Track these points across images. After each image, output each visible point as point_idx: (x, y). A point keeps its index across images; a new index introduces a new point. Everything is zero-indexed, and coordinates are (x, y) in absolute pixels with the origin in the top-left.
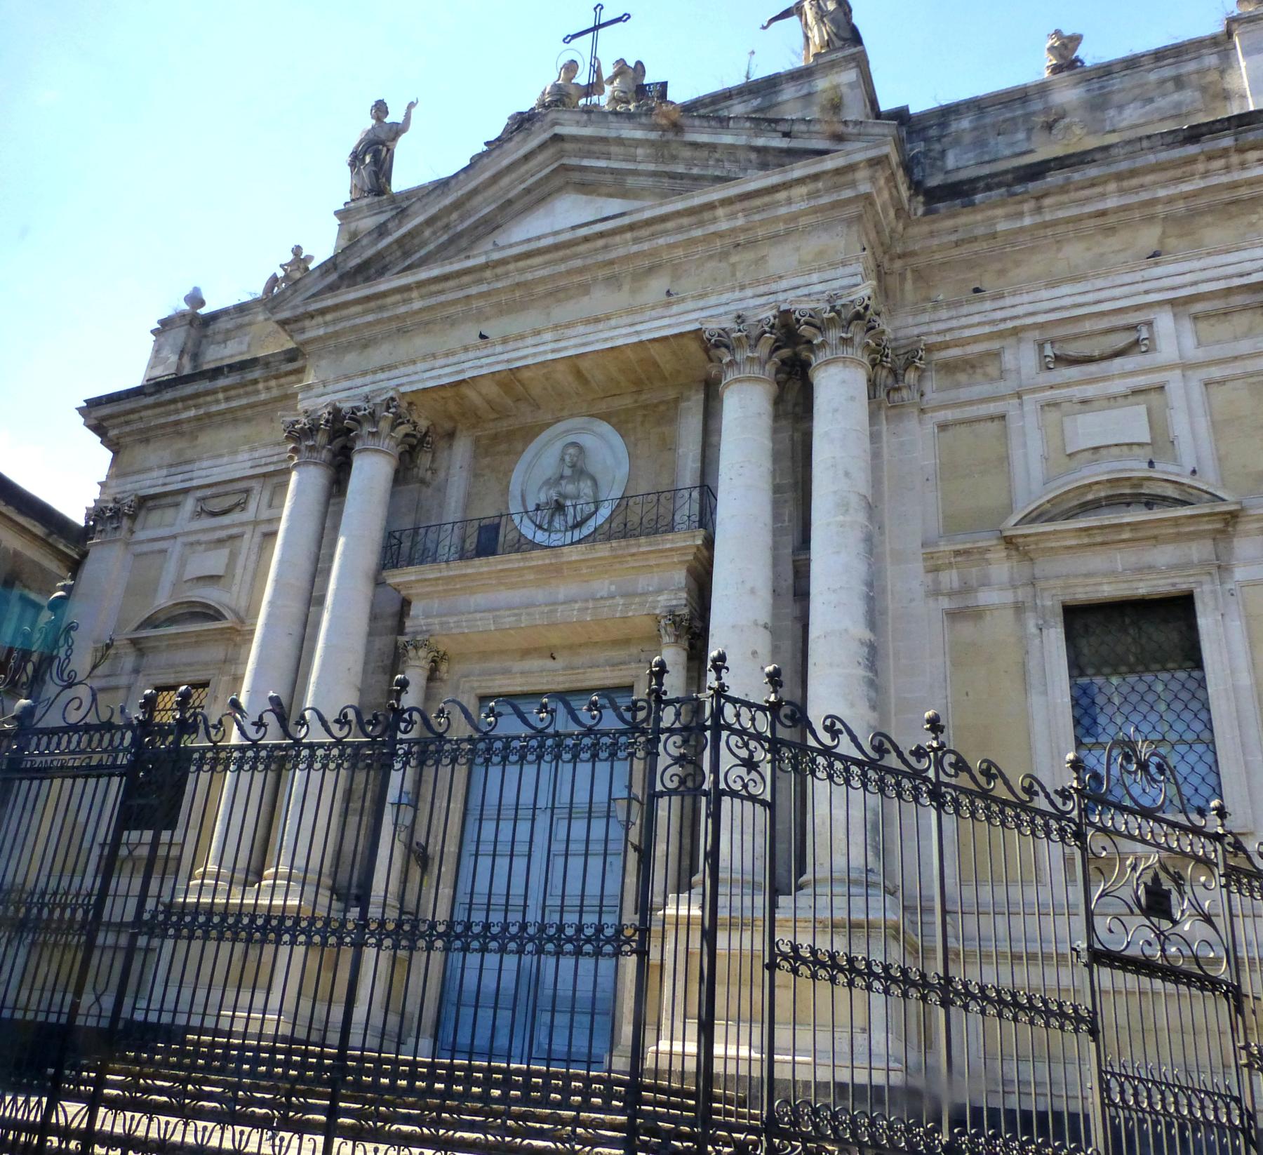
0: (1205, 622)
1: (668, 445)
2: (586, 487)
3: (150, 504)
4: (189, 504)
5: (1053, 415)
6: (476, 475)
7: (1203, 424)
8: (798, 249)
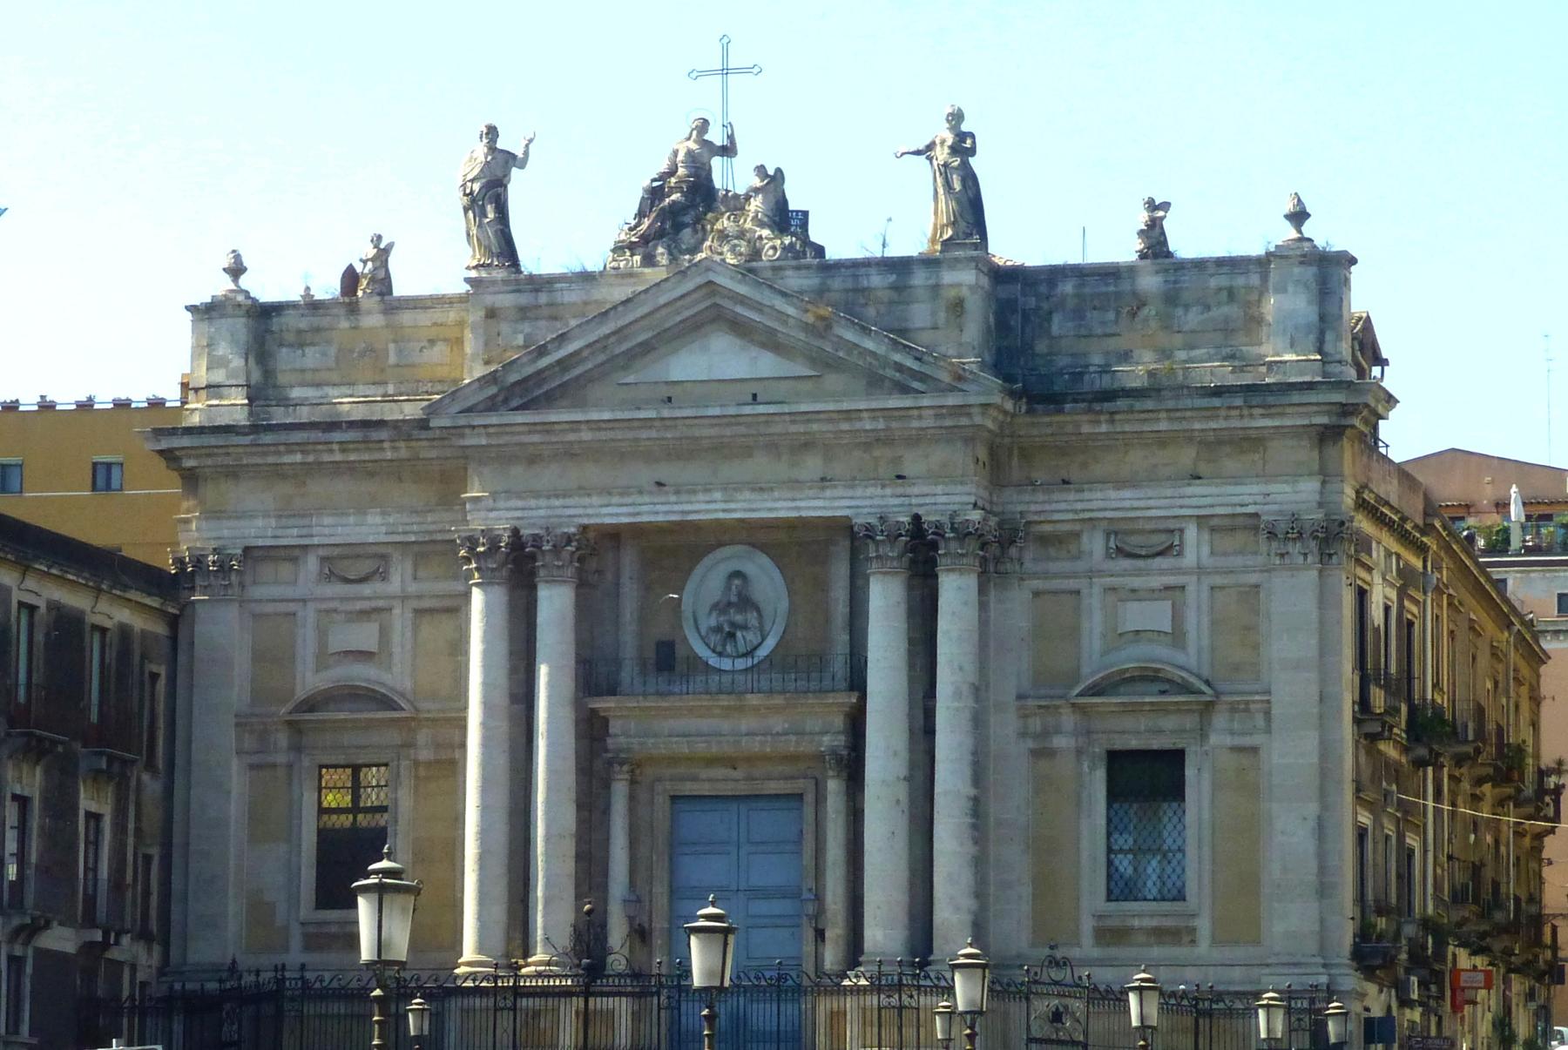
0: (1190, 772)
2: (752, 618)
4: (312, 563)
7: (1205, 620)
8: (927, 457)
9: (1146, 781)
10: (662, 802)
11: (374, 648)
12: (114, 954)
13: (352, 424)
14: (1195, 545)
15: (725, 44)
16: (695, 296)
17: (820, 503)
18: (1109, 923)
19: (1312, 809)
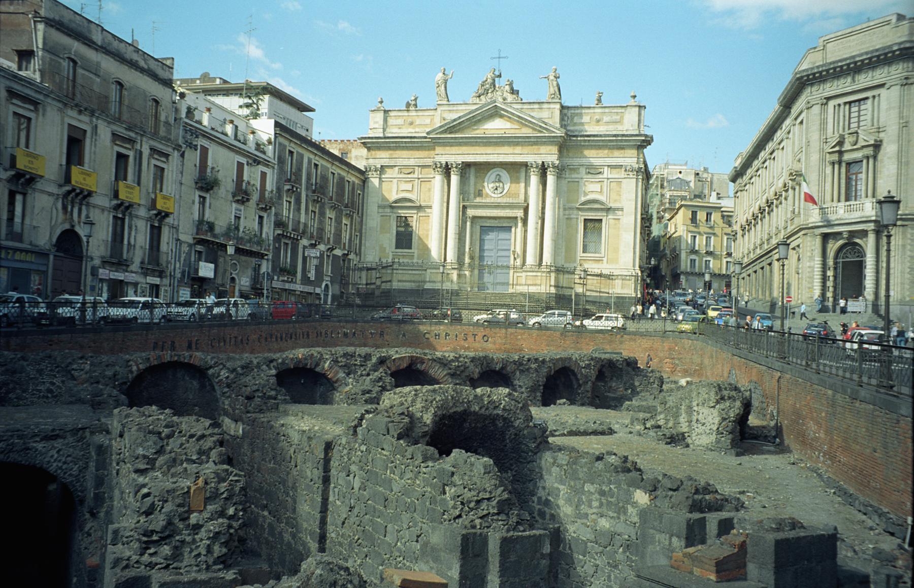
6: (476, 177)
9: (593, 225)
10: (478, 227)
12: (350, 257)
13: (408, 137)
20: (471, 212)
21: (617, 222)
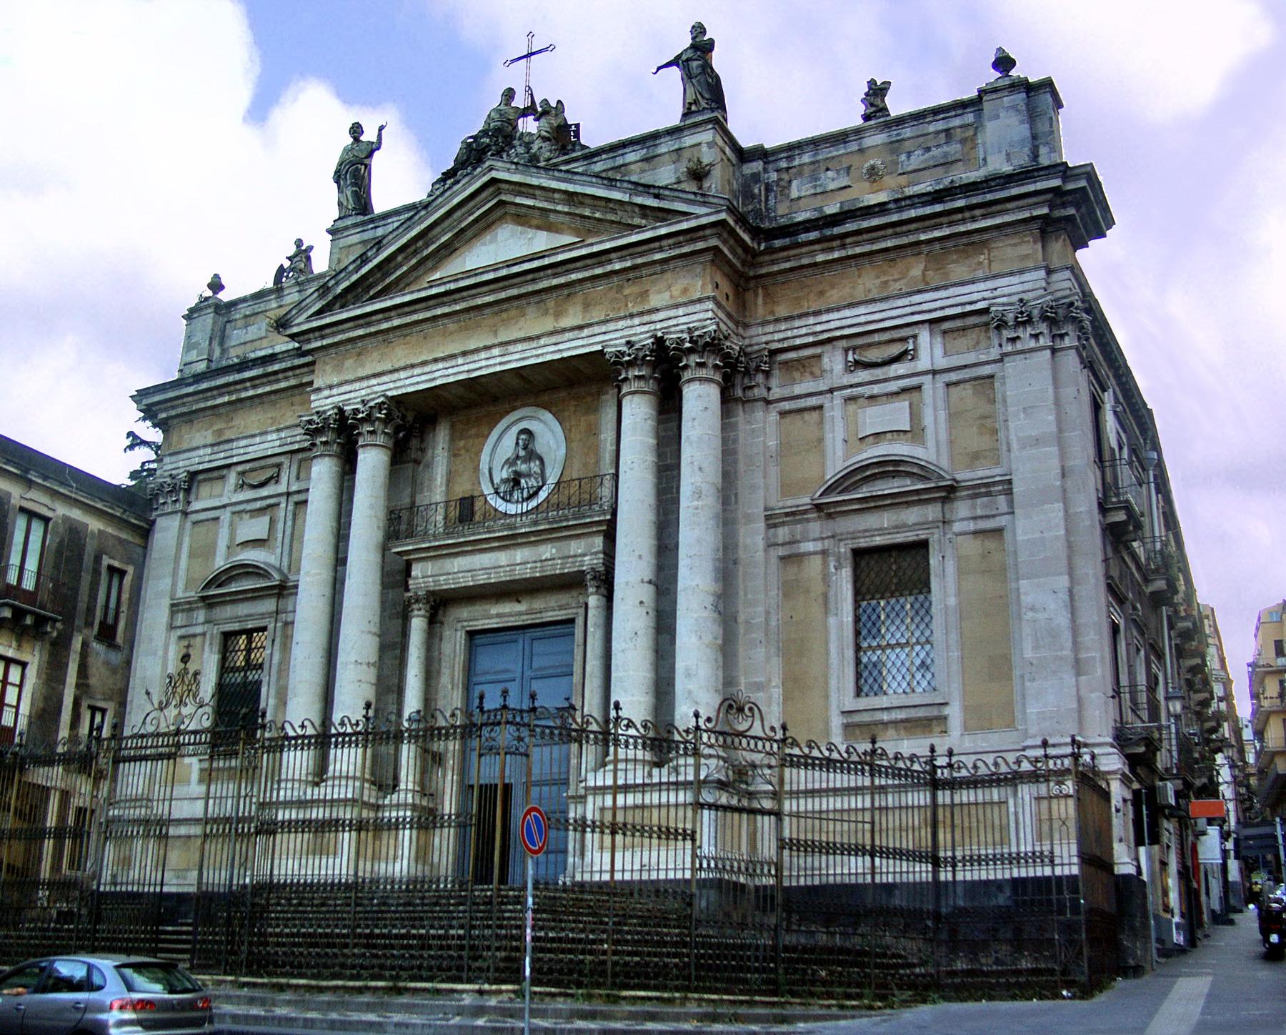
0: (934, 561)
1: (593, 431)
2: (535, 467)
3: (201, 477)
4: (232, 478)
5: (852, 407)
6: (454, 454)
7: (942, 415)
8: (669, 287)
11: (265, 537)
14: (930, 352)
15: (531, 35)
16: (483, 195)
17: (580, 342)
18: (856, 718)
19: (1064, 581)
20: (424, 576)
21: (991, 544)
